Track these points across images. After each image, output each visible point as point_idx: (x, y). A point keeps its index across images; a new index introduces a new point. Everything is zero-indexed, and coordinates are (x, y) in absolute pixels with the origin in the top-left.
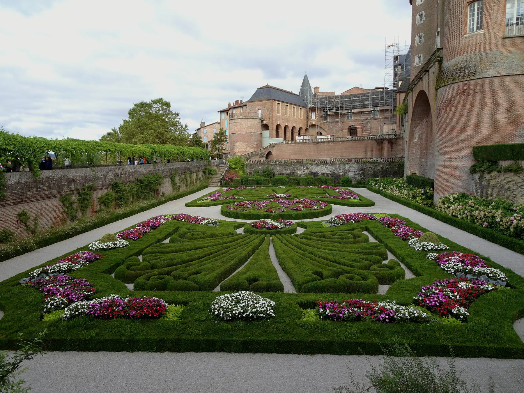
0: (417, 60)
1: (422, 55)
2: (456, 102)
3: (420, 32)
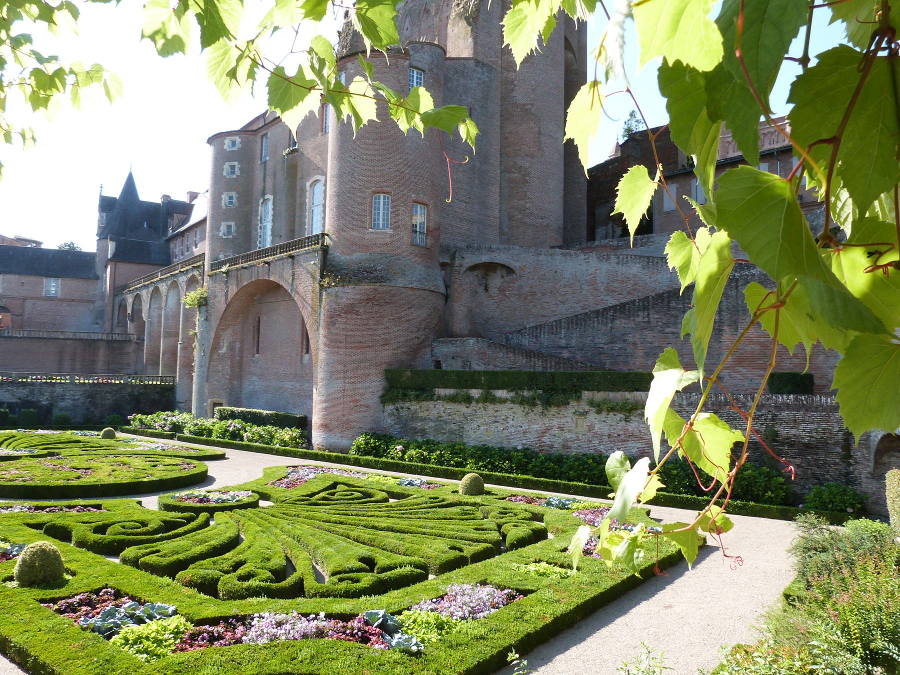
1: (233, 224)
2: (361, 310)
3: (231, 190)
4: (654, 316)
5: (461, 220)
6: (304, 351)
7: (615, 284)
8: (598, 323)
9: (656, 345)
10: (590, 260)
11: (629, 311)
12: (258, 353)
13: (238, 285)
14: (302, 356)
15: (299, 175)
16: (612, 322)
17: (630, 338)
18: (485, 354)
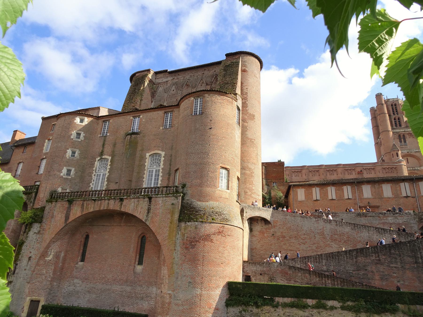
0: (65, 171)
1: (73, 170)
2: (214, 239)
4: (382, 257)
6: (137, 263)
7: (336, 236)
8: (347, 259)
9: (386, 273)
10: (319, 222)
11: (366, 253)
12: (83, 260)
13: (82, 211)
14: (135, 267)
15: (139, 148)
16: (356, 258)
17: (369, 268)
18: (287, 274)
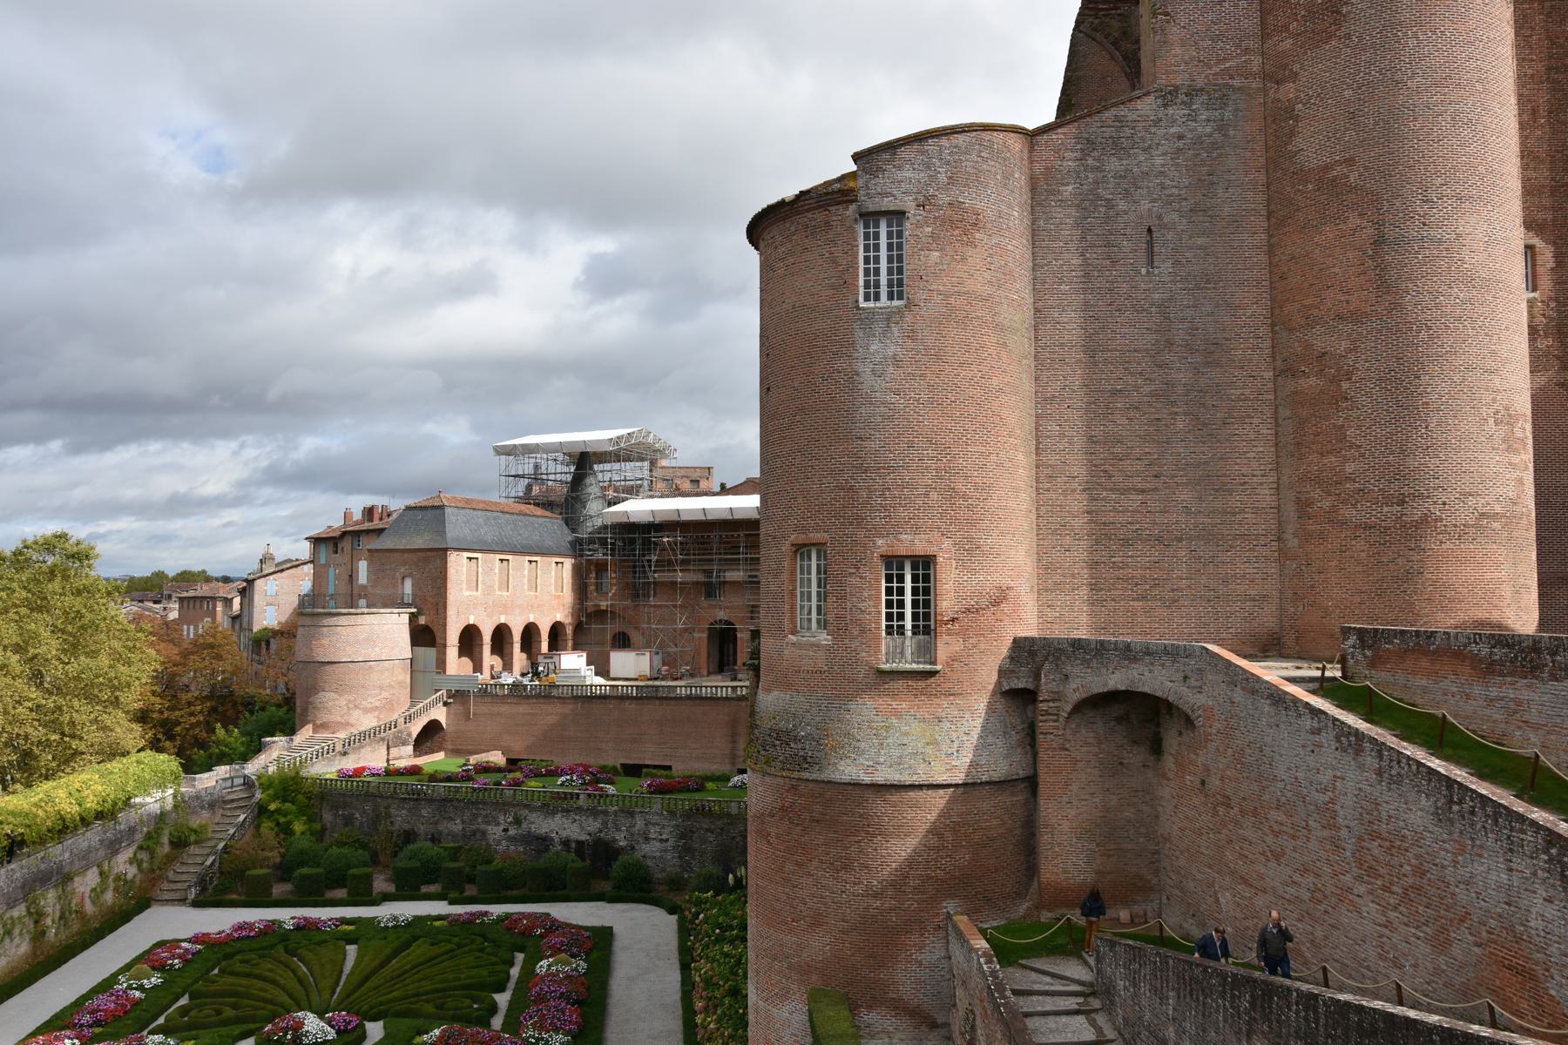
5: (1126, 543)
